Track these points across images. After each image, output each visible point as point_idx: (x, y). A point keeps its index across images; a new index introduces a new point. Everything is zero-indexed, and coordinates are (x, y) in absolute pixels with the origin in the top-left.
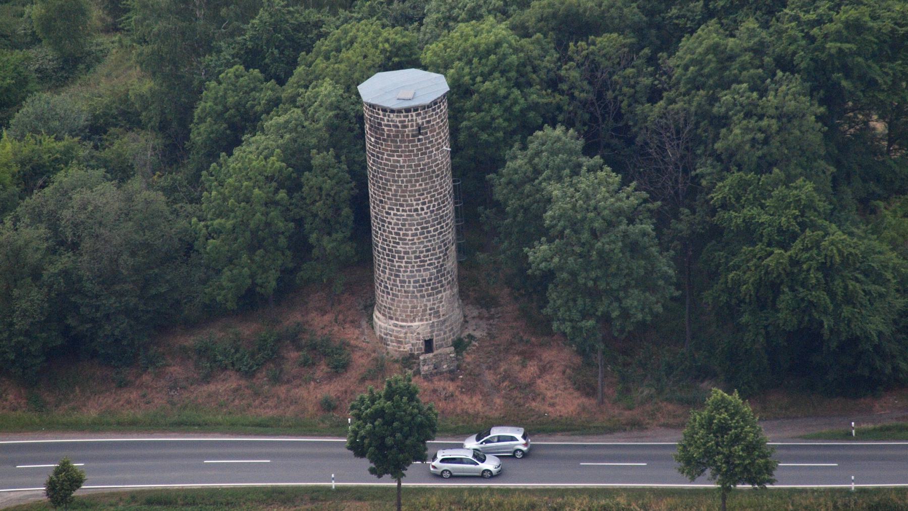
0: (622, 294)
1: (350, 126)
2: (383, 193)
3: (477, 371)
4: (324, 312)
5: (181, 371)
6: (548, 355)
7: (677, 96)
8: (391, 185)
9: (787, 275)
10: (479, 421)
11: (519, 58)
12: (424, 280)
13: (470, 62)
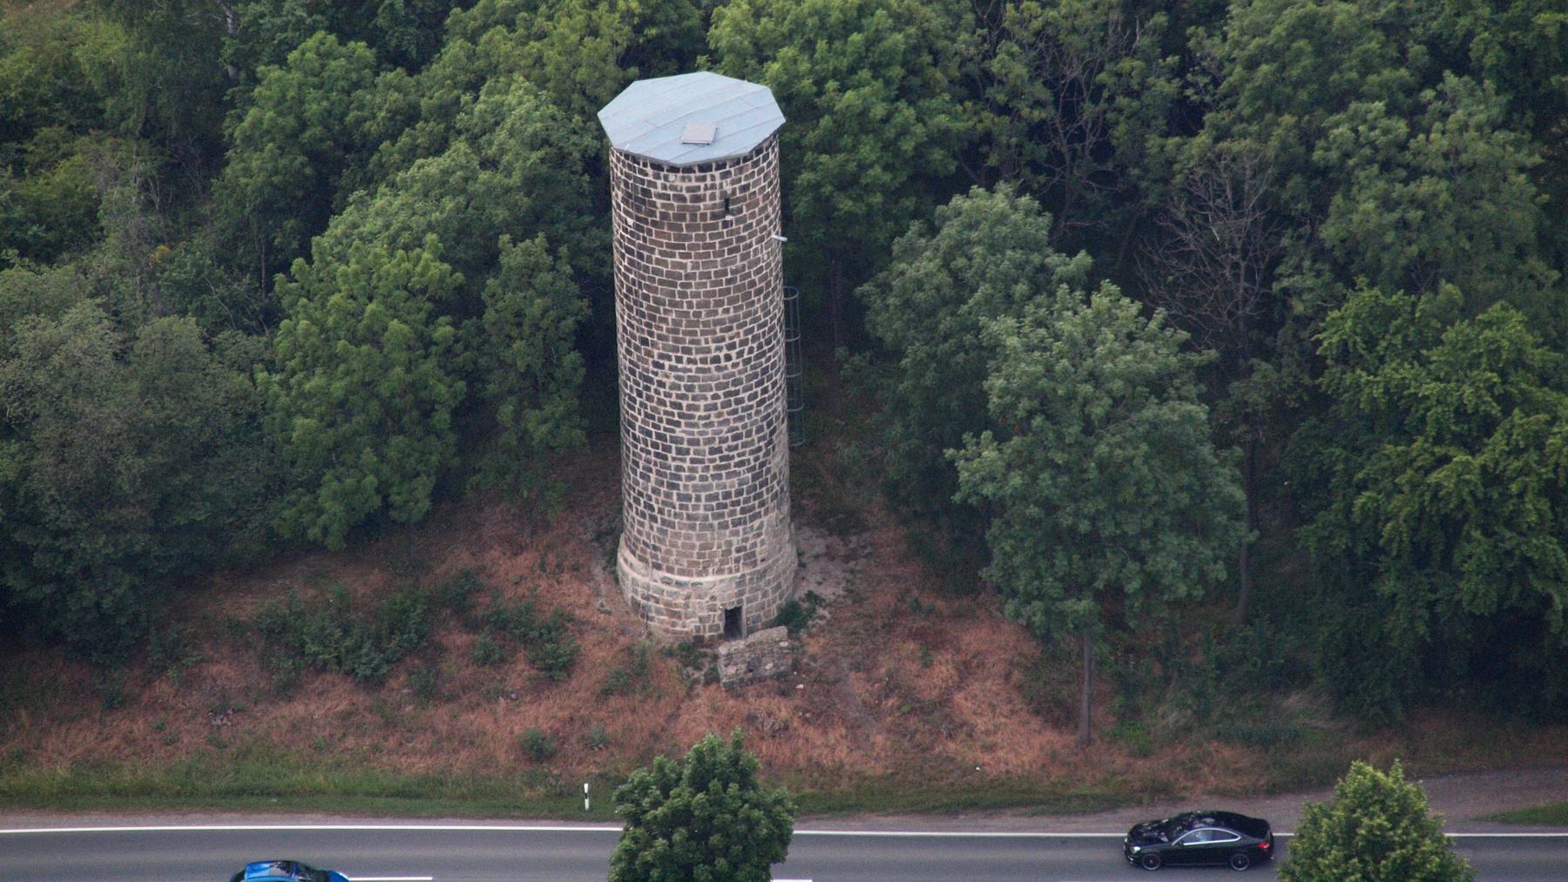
0: (1145, 545)
1: (581, 182)
2: (648, 325)
3: (831, 674)
4: (518, 550)
5: (232, 674)
6: (973, 638)
7: (1234, 122)
8: (666, 311)
9: (1477, 502)
10: (845, 785)
11: (908, 36)
12: (727, 495)
13: (809, 46)
